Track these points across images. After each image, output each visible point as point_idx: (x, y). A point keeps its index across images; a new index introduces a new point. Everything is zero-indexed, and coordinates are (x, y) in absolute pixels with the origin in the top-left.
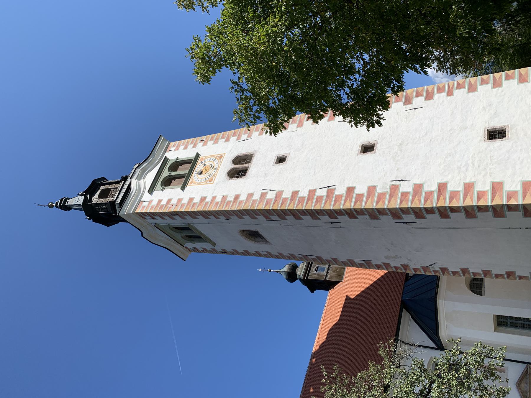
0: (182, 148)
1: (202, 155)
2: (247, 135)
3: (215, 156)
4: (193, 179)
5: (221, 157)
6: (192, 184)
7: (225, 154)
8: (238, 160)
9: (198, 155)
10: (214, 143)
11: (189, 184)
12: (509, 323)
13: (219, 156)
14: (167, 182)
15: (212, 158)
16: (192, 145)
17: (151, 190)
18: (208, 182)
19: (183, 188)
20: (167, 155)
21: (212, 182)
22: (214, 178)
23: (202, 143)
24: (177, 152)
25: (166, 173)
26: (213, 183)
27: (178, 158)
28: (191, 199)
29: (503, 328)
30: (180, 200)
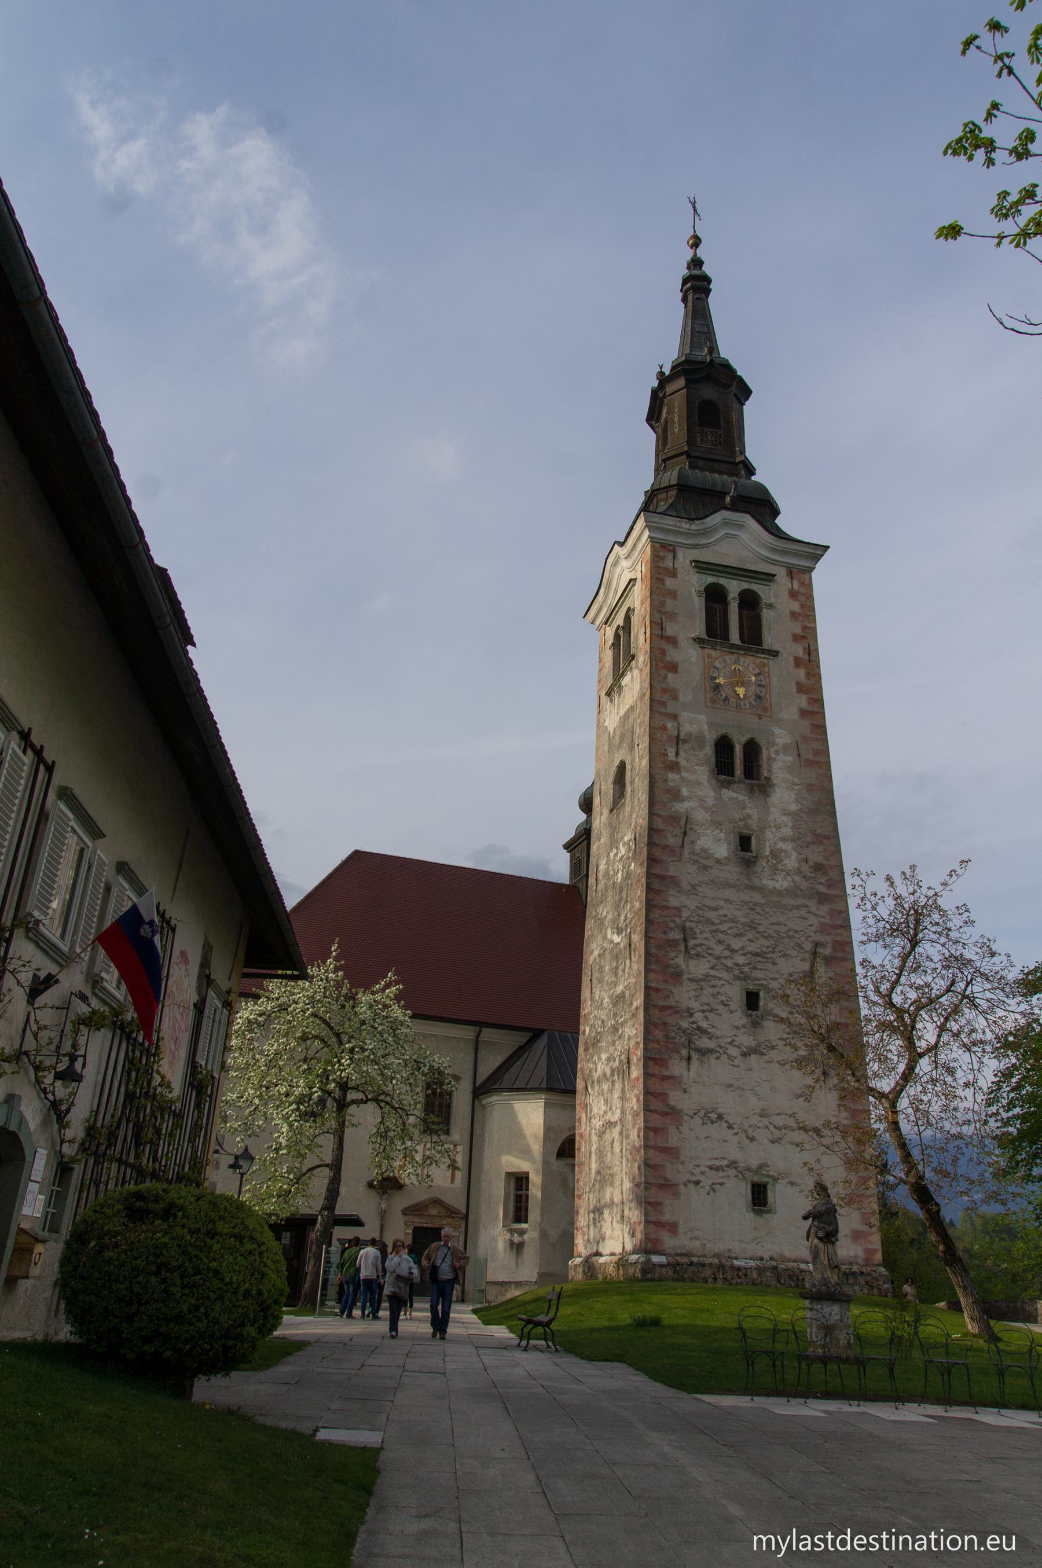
0: (796, 606)
1: (774, 665)
2: (811, 757)
3: (768, 696)
4: (717, 658)
5: (765, 709)
6: (707, 659)
7: (771, 716)
8: (752, 749)
9: (775, 654)
10: (798, 684)
11: (707, 651)
12: (520, 1192)
13: (768, 705)
14: (715, 596)
15: (764, 690)
16: (798, 630)
17: (701, 566)
18: (709, 696)
19: (698, 641)
20: (781, 573)
21: (709, 704)
22: (718, 706)
23: (800, 653)
24: (786, 593)
25: (734, 587)
26: (706, 706)
27: (770, 606)
28: (673, 668)
29: (513, 1185)
30: (673, 641)
